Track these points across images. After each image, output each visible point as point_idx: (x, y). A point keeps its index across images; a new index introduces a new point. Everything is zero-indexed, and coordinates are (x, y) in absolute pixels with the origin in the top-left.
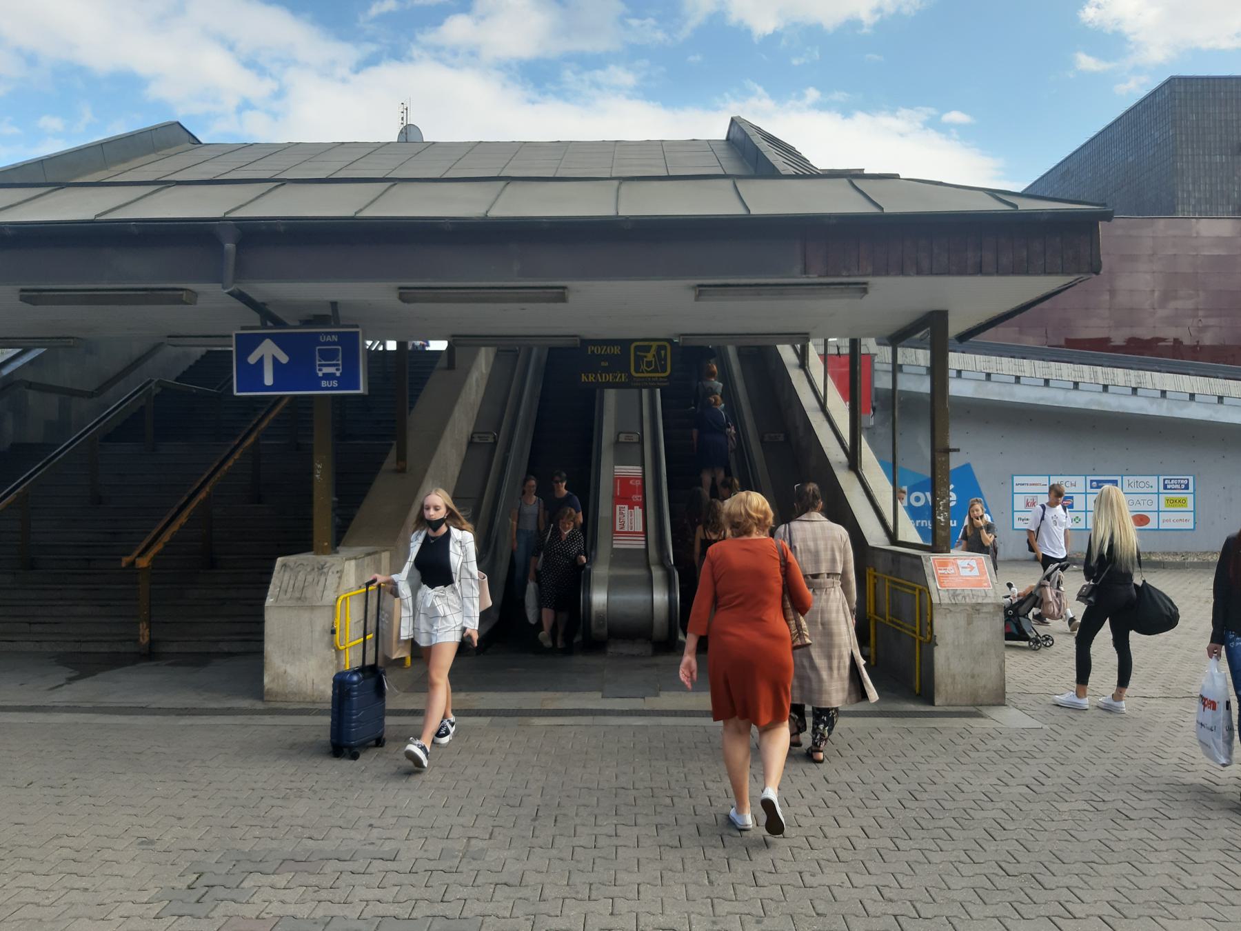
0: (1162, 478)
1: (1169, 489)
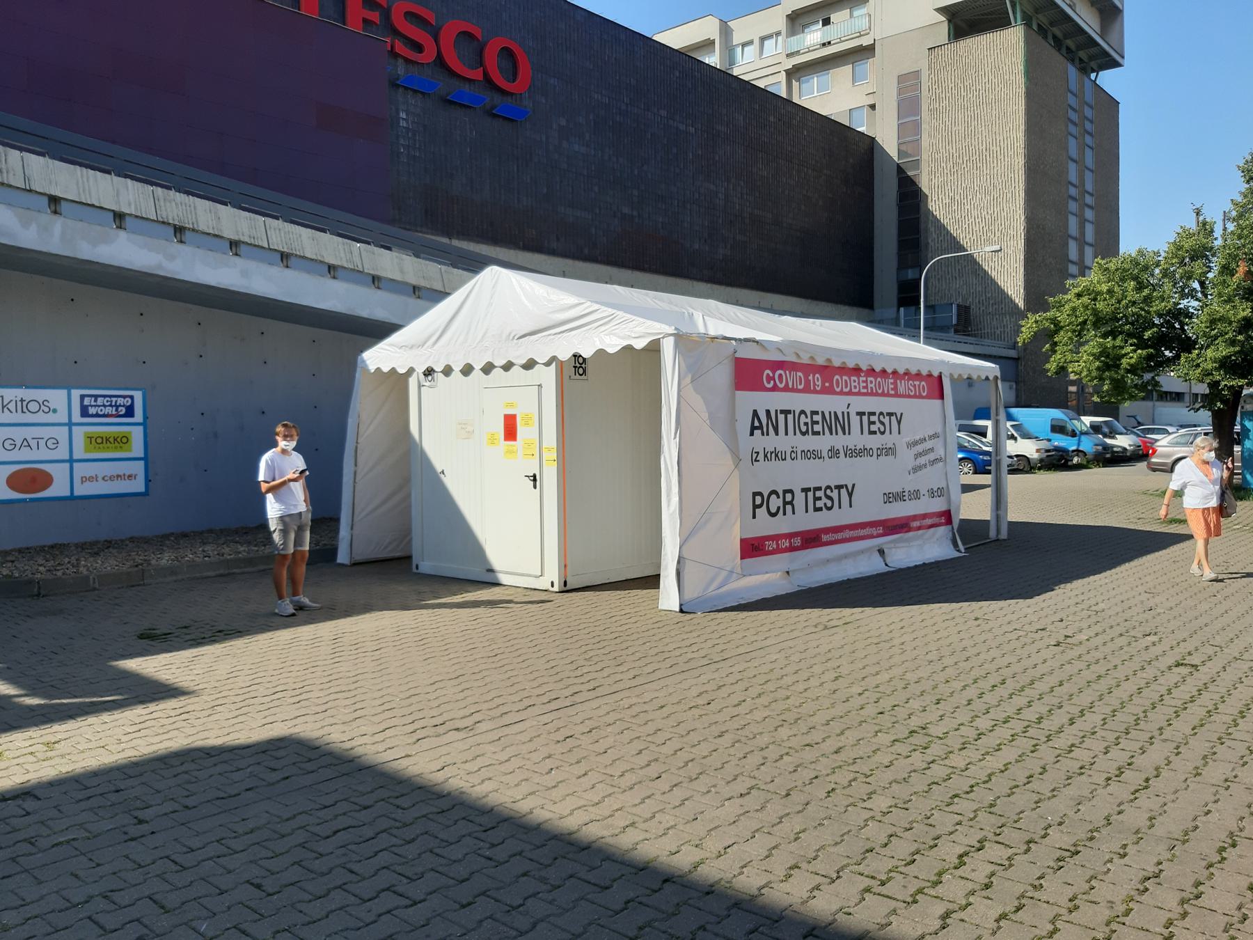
0: (76, 394)
1: (92, 416)
